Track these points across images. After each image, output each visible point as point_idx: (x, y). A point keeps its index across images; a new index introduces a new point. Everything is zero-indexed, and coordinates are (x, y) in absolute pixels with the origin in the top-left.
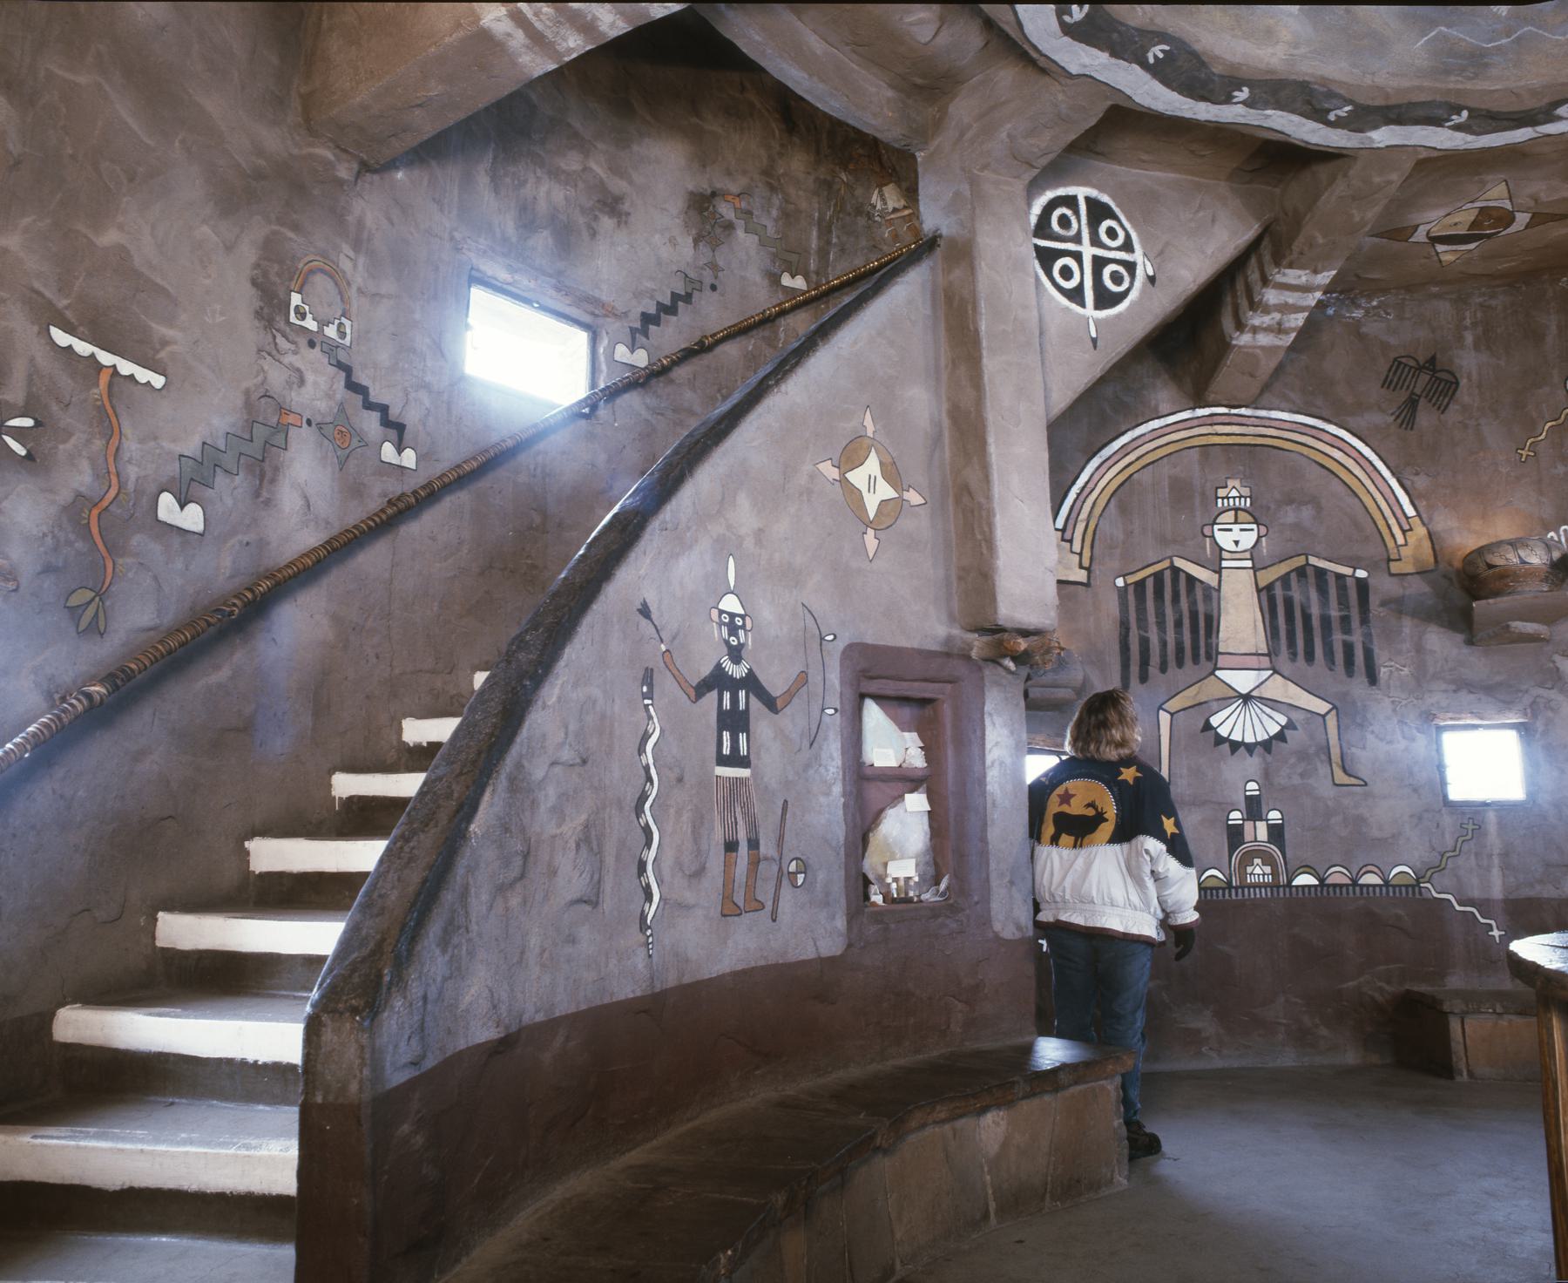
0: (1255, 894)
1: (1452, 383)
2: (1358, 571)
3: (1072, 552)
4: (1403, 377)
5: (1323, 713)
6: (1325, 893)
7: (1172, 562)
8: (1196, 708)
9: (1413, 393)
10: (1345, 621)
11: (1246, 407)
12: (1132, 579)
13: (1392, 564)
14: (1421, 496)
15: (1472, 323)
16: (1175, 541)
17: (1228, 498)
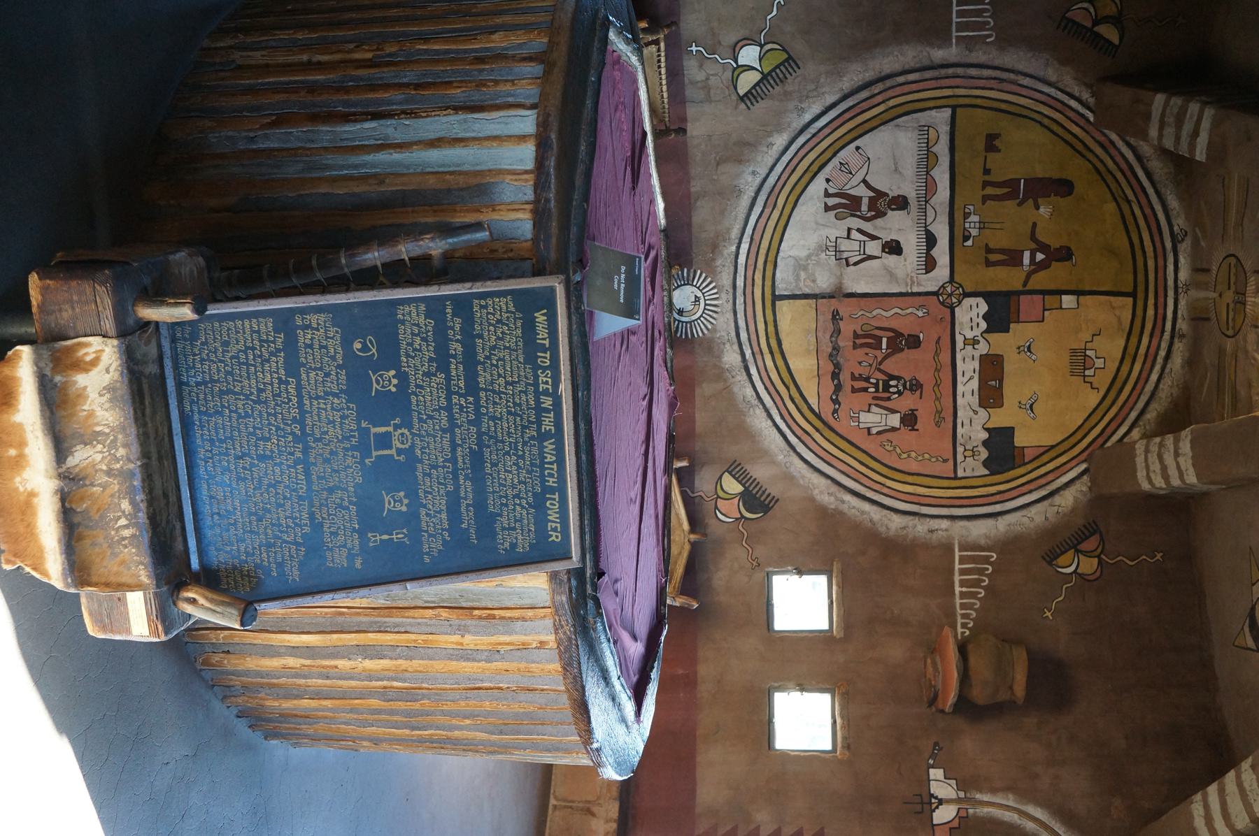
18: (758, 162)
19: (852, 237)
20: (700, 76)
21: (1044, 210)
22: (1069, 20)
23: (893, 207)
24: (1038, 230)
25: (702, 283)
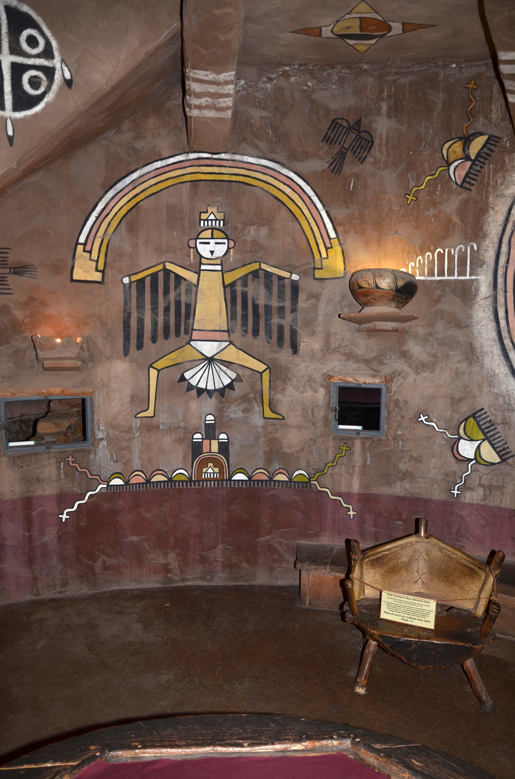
0: (207, 486)
1: (369, 141)
3: (91, 259)
5: (261, 371)
6: (252, 485)
7: (164, 266)
8: (175, 366)
9: (342, 147)
10: (281, 310)
11: (225, 153)
12: (135, 278)
13: (316, 271)
14: (340, 224)
16: (168, 251)
22: (464, 181)
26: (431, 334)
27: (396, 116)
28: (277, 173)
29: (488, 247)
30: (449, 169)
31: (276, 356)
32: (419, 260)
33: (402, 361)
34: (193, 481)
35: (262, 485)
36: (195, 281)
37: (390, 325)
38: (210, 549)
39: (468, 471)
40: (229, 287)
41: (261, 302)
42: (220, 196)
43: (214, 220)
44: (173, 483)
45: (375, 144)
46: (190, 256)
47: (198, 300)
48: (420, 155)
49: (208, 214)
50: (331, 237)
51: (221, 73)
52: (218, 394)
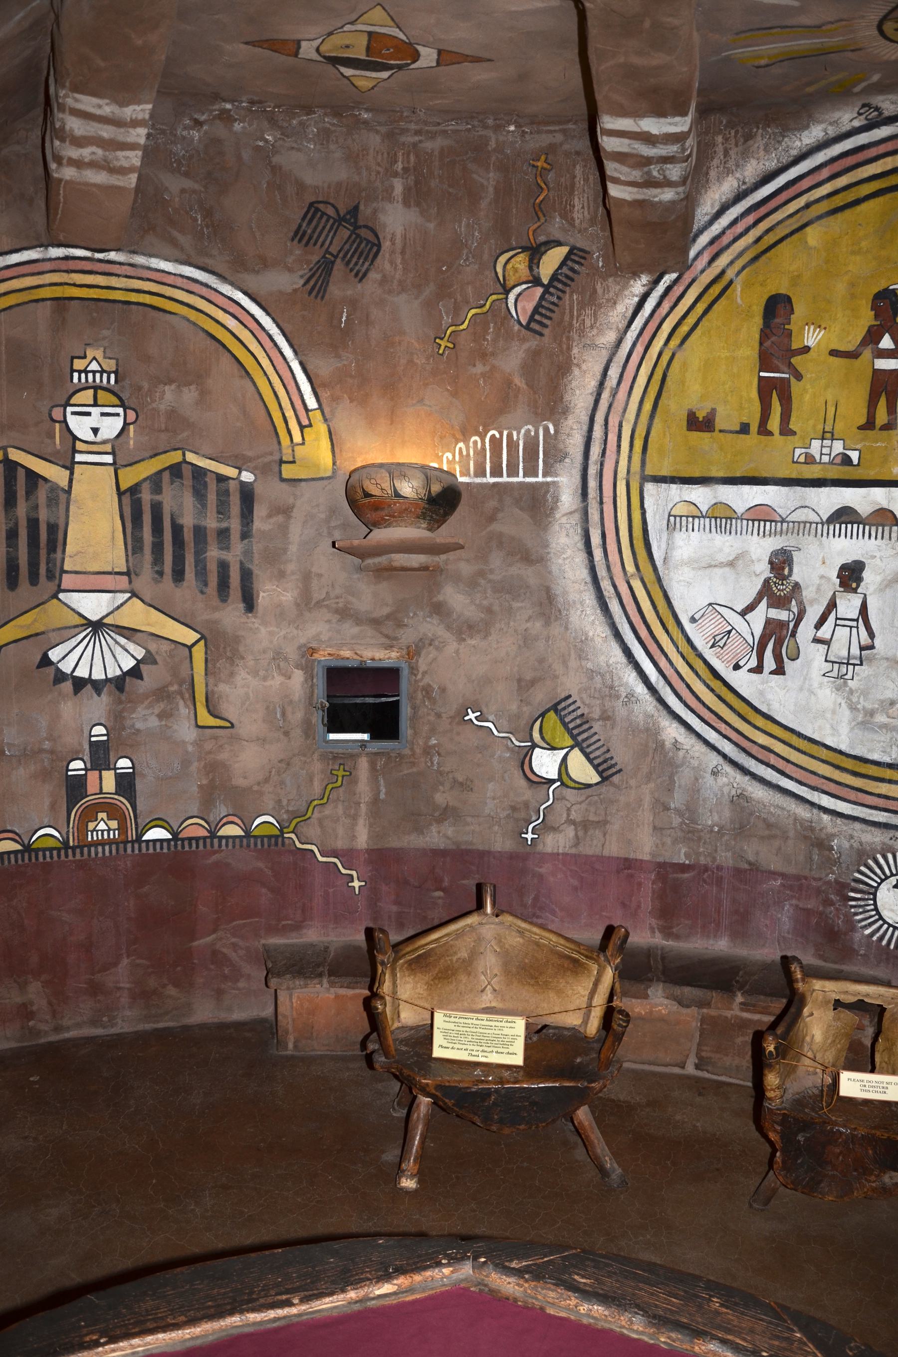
0: (97, 854)
1: (374, 244)
2: (244, 473)
4: (318, 230)
5: (189, 644)
6: (179, 848)
8: (31, 639)
10: (223, 534)
11: (117, 250)
13: (284, 466)
14: (324, 385)
15: (403, 168)
17: (86, 372)
18: (700, 764)
19: (827, 636)
20: (570, 832)
21: (812, 338)
22: (531, 319)
23: (786, 572)
24: (842, 348)
25: (875, 874)
26: (481, 573)
27: (418, 204)
28: (213, 292)
29: (572, 429)
30: (507, 298)
31: (217, 615)
32: (460, 449)
33: (435, 620)
34: (70, 848)
35: (197, 847)
36: (64, 483)
37: (416, 560)
38: (105, 968)
39: (548, 800)
40: (128, 494)
41: (188, 521)
42: (108, 329)
43: (98, 371)
44: (33, 855)
45: (383, 249)
46: (55, 437)
47: (71, 518)
48: (459, 273)
49: (86, 361)
50: (310, 408)
51: (127, 105)
52: (113, 687)
